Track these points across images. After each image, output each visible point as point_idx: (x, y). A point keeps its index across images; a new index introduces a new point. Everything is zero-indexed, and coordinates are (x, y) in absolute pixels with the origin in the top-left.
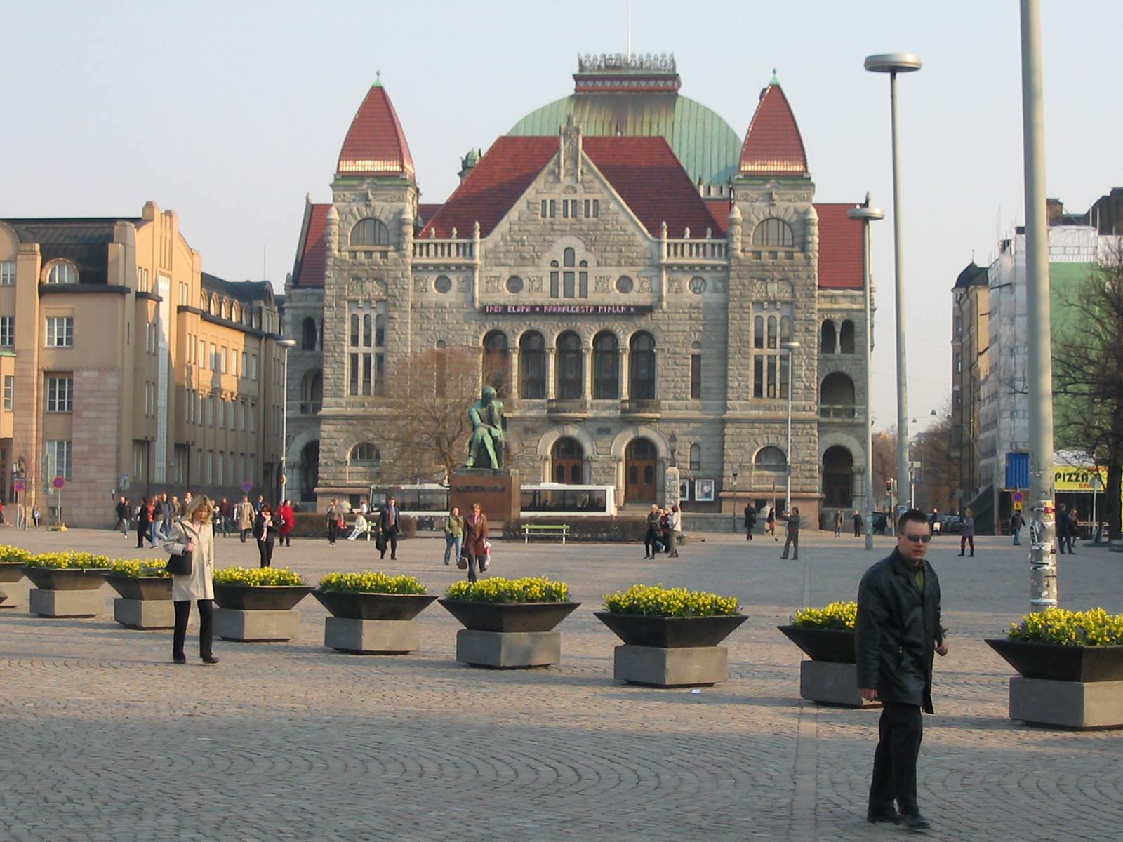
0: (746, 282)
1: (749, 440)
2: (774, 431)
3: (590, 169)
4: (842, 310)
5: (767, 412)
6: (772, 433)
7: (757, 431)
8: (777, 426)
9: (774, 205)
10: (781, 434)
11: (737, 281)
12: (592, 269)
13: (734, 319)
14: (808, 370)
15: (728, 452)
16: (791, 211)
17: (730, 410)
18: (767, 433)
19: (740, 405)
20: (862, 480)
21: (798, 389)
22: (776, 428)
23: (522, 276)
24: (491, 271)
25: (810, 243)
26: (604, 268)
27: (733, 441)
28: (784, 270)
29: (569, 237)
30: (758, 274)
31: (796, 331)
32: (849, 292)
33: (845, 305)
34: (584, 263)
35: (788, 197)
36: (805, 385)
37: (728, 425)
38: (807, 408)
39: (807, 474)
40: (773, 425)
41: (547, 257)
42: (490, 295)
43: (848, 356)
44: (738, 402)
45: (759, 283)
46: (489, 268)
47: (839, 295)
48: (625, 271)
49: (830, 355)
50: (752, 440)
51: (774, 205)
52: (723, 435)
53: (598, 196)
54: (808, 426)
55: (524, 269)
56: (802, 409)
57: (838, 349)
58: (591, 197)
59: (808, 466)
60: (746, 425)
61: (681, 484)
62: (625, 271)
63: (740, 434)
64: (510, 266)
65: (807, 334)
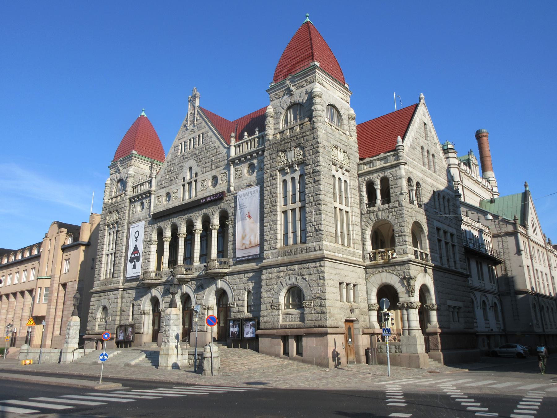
0: (274, 156)
1: (277, 282)
2: (294, 272)
3: (201, 116)
4: (377, 171)
5: (289, 257)
6: (292, 274)
7: (282, 274)
8: (296, 267)
9: (292, 95)
10: (299, 275)
11: (269, 158)
12: (200, 178)
13: (267, 186)
14: (316, 214)
15: (264, 295)
16: (303, 94)
17: (265, 259)
18: (289, 275)
19: (272, 253)
20: (408, 314)
21: (310, 232)
22: (295, 270)
23: (170, 192)
24: (159, 193)
25: (313, 111)
26: (204, 175)
27: (267, 285)
28: (297, 138)
29: (190, 160)
30: (282, 148)
31: (306, 184)
32: (382, 155)
33: (379, 164)
34: (196, 174)
35: (301, 84)
36: (315, 228)
37: (264, 272)
38: (317, 248)
39: (318, 309)
40: (292, 267)
41: (181, 176)
42: (158, 207)
43: (386, 206)
44: (270, 251)
45: (283, 154)
46: (158, 191)
47: (375, 160)
48: (214, 173)
49: (371, 209)
50: (279, 282)
51: (292, 95)
52: (260, 280)
53: (203, 131)
54: (318, 264)
55: (170, 187)
56: (313, 250)
57: (379, 202)
58: (200, 132)
59: (319, 302)
60: (275, 270)
61: (348, 326)
62: (214, 173)
63: (271, 279)
64: (166, 187)
65: (314, 184)
